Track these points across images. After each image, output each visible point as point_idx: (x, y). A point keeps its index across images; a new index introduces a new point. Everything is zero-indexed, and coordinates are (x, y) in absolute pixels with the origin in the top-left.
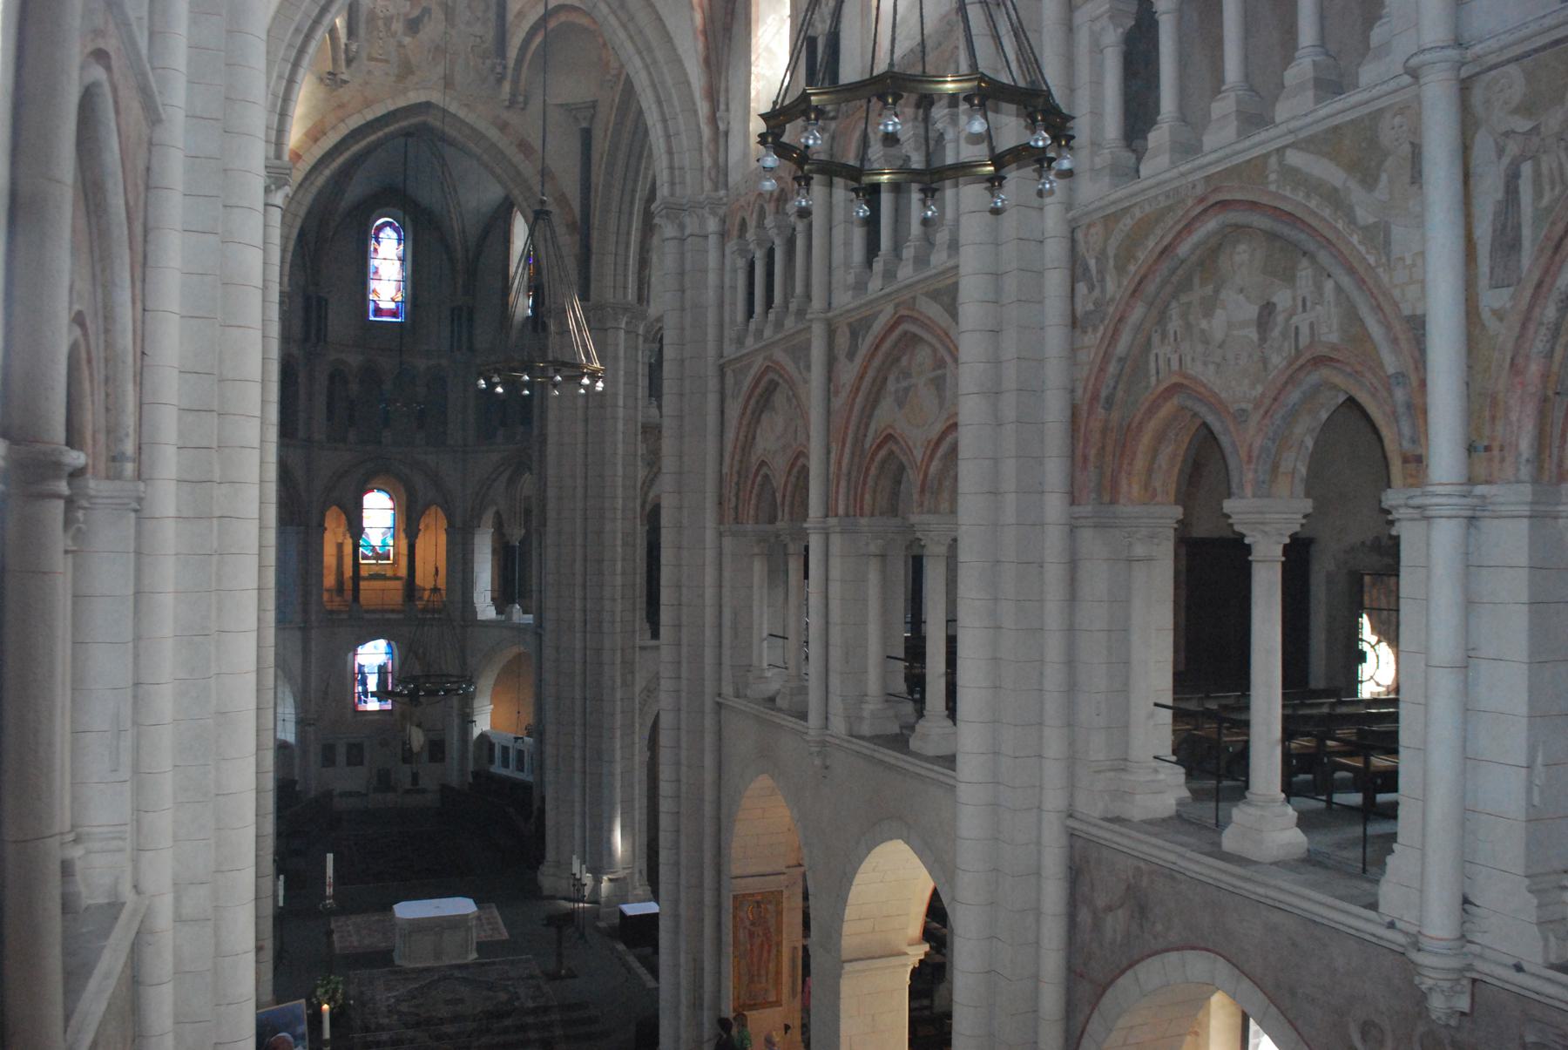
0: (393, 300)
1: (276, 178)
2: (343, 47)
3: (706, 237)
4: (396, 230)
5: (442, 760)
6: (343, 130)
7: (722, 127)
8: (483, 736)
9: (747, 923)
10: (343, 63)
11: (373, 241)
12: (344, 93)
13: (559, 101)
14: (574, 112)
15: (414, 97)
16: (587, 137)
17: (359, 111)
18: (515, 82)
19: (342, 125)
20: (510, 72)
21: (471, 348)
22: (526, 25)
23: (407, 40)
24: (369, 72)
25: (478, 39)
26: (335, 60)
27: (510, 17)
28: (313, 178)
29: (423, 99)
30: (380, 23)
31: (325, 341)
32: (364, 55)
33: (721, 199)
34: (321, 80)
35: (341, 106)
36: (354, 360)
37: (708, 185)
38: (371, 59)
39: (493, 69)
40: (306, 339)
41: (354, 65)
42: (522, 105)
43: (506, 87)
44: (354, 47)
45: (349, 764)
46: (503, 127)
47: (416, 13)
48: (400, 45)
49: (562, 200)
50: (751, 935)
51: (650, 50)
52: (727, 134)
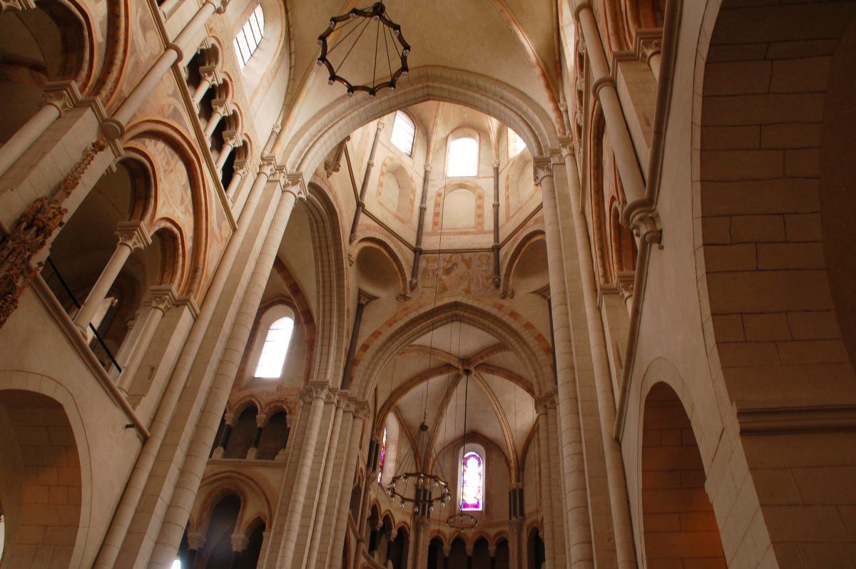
0: (475, 498)
3: (565, 164)
6: (406, 319)
7: (562, 109)
10: (408, 290)
12: (409, 303)
13: (533, 290)
15: (447, 300)
17: (417, 310)
20: (502, 282)
22: (509, 256)
23: (444, 277)
24: (423, 293)
26: (405, 289)
27: (500, 259)
28: (388, 346)
29: (453, 300)
30: (430, 273)
32: (420, 286)
33: (568, 138)
34: (397, 298)
35: (406, 309)
36: (447, 531)
37: (559, 135)
38: (424, 287)
39: (494, 282)
41: (415, 290)
43: (501, 288)
44: (414, 281)
46: (500, 307)
47: (449, 265)
48: (441, 280)
49: (540, 337)
51: (519, 108)
52: (567, 111)
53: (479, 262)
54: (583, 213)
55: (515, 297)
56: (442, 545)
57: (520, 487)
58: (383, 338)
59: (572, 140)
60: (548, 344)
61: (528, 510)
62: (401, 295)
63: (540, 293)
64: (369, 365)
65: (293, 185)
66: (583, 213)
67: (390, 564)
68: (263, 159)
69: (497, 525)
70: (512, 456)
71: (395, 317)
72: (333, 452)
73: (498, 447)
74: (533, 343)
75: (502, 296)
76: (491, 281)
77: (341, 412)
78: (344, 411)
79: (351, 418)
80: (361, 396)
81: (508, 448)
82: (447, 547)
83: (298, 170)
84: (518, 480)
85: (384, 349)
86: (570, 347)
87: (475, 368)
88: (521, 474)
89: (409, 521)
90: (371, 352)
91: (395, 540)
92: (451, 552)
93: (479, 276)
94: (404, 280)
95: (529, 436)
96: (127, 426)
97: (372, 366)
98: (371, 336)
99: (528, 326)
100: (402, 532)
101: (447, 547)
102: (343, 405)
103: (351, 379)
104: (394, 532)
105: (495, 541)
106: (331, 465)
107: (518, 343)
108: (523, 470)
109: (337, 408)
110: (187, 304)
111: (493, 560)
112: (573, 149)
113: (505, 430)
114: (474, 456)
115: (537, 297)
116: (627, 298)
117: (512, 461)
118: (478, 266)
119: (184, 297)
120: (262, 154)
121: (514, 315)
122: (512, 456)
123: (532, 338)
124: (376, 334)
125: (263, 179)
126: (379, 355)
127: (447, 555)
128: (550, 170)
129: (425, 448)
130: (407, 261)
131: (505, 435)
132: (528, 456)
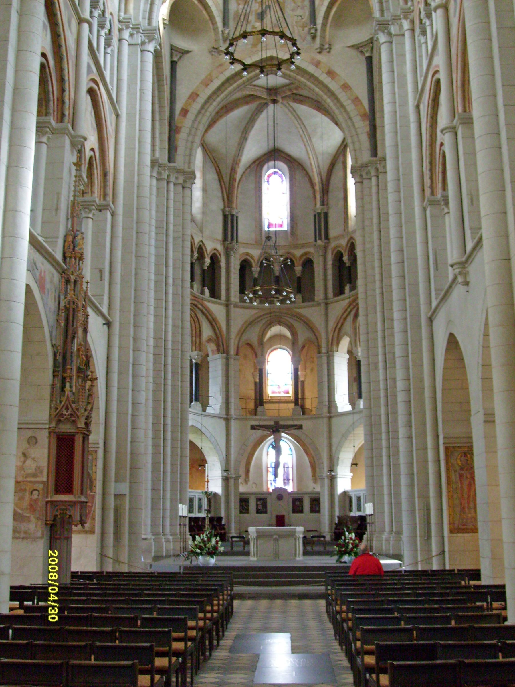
1: (148, 36)
2: (221, 32)
3: (403, 35)
4: (281, 177)
5: (319, 511)
6: (222, 78)
8: (345, 493)
9: (458, 468)
11: (266, 183)
13: (351, 44)
14: (360, 49)
16: (369, 60)
18: (323, 37)
19: (221, 76)
20: (319, 34)
21: (327, 237)
25: (300, 18)
28: (206, 107)
31: (237, 241)
33: (410, 9)
34: (210, 52)
36: (256, 253)
39: (309, 32)
40: (225, 239)
42: (328, 50)
43: (318, 40)
44: (227, 31)
45: (258, 511)
46: (317, 64)
49: (356, 100)
50: (461, 476)
53: (293, 4)
54: (418, 107)
55: (332, 52)
56: (251, 266)
57: (325, 211)
58: (201, 101)
59: (413, 11)
60: (365, 109)
61: (332, 233)
62: (214, 48)
63: (358, 48)
64: (190, 130)
65: (150, 41)
66: (418, 107)
67: (207, 291)
68: (120, 22)
69: (303, 246)
70: (316, 180)
71: (210, 74)
72: (171, 227)
73: (302, 166)
74: (350, 107)
75: (319, 50)
76: (306, 29)
77: (171, 186)
78: (174, 184)
79: (181, 188)
80: (187, 165)
81: (313, 171)
82: (256, 269)
83: (150, 24)
84: (323, 204)
85: (203, 111)
86: (401, 232)
87: (282, 98)
88: (325, 196)
89: (220, 248)
90: (191, 116)
91: (208, 267)
92: (260, 273)
93: (294, 23)
94: (216, 29)
95: (334, 157)
96: (104, 324)
97: (193, 130)
98: (189, 98)
99: (346, 87)
100: (214, 258)
101: (256, 269)
102: (172, 179)
103: (176, 149)
104: (208, 261)
105: (301, 262)
106: (171, 240)
107: (335, 105)
108: (328, 192)
109: (168, 183)
110: (108, 209)
111: (299, 278)
112: (412, 22)
113: (310, 153)
114: (275, 173)
115: (354, 53)
116: (445, 214)
117: (317, 184)
118: (293, 10)
119: (103, 203)
120: (119, 16)
121: (331, 73)
122: (316, 180)
123: (349, 102)
124: (194, 96)
125: (125, 44)
126: (199, 118)
127: (256, 276)
128: (390, 34)
129: (229, 171)
130: (217, 5)
131: (310, 158)
132: (332, 178)
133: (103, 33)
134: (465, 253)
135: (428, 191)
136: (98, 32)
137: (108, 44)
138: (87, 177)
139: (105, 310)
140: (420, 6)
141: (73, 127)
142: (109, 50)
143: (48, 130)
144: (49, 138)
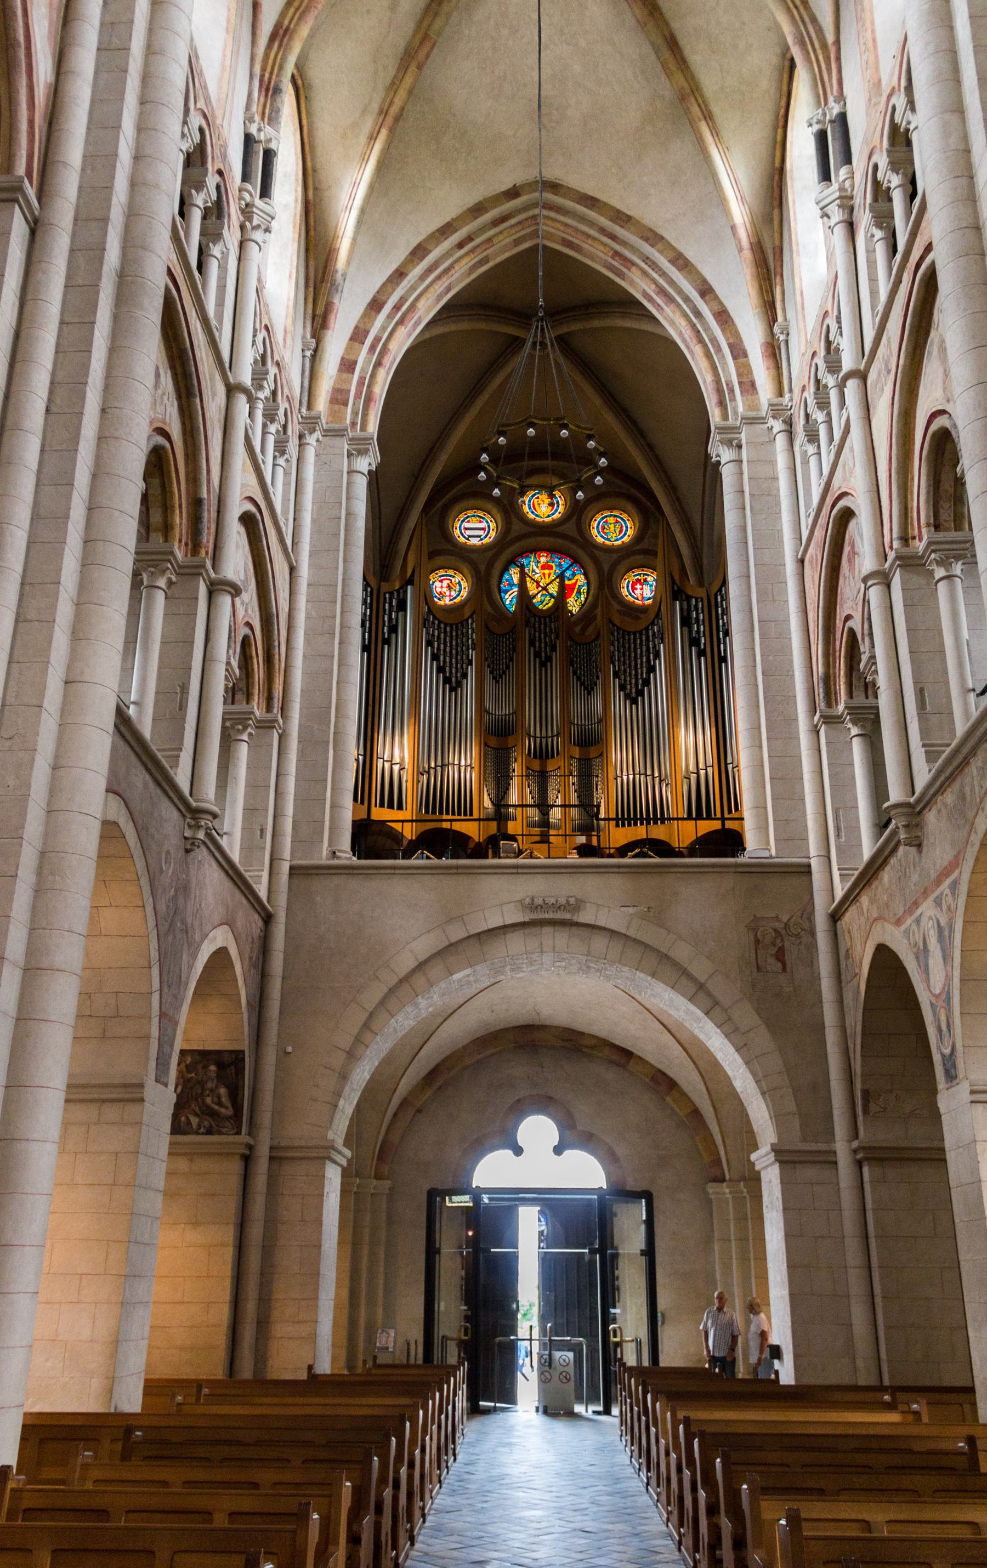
112: (789, 423)
133: (273, 428)
134: (913, 793)
135: (821, 703)
136: (265, 426)
137: (281, 449)
138: (239, 667)
139: (263, 893)
140: (806, 394)
141: (213, 568)
142: (281, 461)
143: (169, 566)
144: (170, 583)
